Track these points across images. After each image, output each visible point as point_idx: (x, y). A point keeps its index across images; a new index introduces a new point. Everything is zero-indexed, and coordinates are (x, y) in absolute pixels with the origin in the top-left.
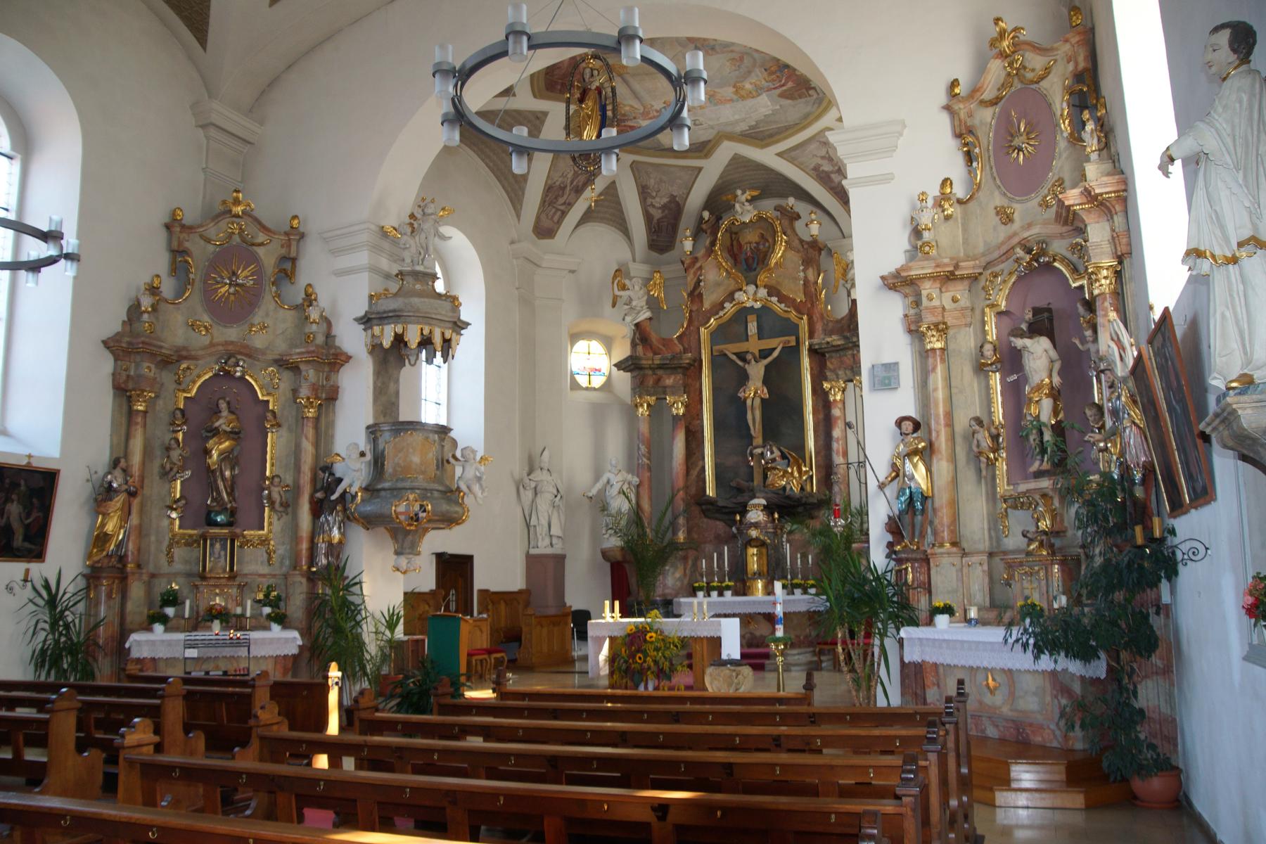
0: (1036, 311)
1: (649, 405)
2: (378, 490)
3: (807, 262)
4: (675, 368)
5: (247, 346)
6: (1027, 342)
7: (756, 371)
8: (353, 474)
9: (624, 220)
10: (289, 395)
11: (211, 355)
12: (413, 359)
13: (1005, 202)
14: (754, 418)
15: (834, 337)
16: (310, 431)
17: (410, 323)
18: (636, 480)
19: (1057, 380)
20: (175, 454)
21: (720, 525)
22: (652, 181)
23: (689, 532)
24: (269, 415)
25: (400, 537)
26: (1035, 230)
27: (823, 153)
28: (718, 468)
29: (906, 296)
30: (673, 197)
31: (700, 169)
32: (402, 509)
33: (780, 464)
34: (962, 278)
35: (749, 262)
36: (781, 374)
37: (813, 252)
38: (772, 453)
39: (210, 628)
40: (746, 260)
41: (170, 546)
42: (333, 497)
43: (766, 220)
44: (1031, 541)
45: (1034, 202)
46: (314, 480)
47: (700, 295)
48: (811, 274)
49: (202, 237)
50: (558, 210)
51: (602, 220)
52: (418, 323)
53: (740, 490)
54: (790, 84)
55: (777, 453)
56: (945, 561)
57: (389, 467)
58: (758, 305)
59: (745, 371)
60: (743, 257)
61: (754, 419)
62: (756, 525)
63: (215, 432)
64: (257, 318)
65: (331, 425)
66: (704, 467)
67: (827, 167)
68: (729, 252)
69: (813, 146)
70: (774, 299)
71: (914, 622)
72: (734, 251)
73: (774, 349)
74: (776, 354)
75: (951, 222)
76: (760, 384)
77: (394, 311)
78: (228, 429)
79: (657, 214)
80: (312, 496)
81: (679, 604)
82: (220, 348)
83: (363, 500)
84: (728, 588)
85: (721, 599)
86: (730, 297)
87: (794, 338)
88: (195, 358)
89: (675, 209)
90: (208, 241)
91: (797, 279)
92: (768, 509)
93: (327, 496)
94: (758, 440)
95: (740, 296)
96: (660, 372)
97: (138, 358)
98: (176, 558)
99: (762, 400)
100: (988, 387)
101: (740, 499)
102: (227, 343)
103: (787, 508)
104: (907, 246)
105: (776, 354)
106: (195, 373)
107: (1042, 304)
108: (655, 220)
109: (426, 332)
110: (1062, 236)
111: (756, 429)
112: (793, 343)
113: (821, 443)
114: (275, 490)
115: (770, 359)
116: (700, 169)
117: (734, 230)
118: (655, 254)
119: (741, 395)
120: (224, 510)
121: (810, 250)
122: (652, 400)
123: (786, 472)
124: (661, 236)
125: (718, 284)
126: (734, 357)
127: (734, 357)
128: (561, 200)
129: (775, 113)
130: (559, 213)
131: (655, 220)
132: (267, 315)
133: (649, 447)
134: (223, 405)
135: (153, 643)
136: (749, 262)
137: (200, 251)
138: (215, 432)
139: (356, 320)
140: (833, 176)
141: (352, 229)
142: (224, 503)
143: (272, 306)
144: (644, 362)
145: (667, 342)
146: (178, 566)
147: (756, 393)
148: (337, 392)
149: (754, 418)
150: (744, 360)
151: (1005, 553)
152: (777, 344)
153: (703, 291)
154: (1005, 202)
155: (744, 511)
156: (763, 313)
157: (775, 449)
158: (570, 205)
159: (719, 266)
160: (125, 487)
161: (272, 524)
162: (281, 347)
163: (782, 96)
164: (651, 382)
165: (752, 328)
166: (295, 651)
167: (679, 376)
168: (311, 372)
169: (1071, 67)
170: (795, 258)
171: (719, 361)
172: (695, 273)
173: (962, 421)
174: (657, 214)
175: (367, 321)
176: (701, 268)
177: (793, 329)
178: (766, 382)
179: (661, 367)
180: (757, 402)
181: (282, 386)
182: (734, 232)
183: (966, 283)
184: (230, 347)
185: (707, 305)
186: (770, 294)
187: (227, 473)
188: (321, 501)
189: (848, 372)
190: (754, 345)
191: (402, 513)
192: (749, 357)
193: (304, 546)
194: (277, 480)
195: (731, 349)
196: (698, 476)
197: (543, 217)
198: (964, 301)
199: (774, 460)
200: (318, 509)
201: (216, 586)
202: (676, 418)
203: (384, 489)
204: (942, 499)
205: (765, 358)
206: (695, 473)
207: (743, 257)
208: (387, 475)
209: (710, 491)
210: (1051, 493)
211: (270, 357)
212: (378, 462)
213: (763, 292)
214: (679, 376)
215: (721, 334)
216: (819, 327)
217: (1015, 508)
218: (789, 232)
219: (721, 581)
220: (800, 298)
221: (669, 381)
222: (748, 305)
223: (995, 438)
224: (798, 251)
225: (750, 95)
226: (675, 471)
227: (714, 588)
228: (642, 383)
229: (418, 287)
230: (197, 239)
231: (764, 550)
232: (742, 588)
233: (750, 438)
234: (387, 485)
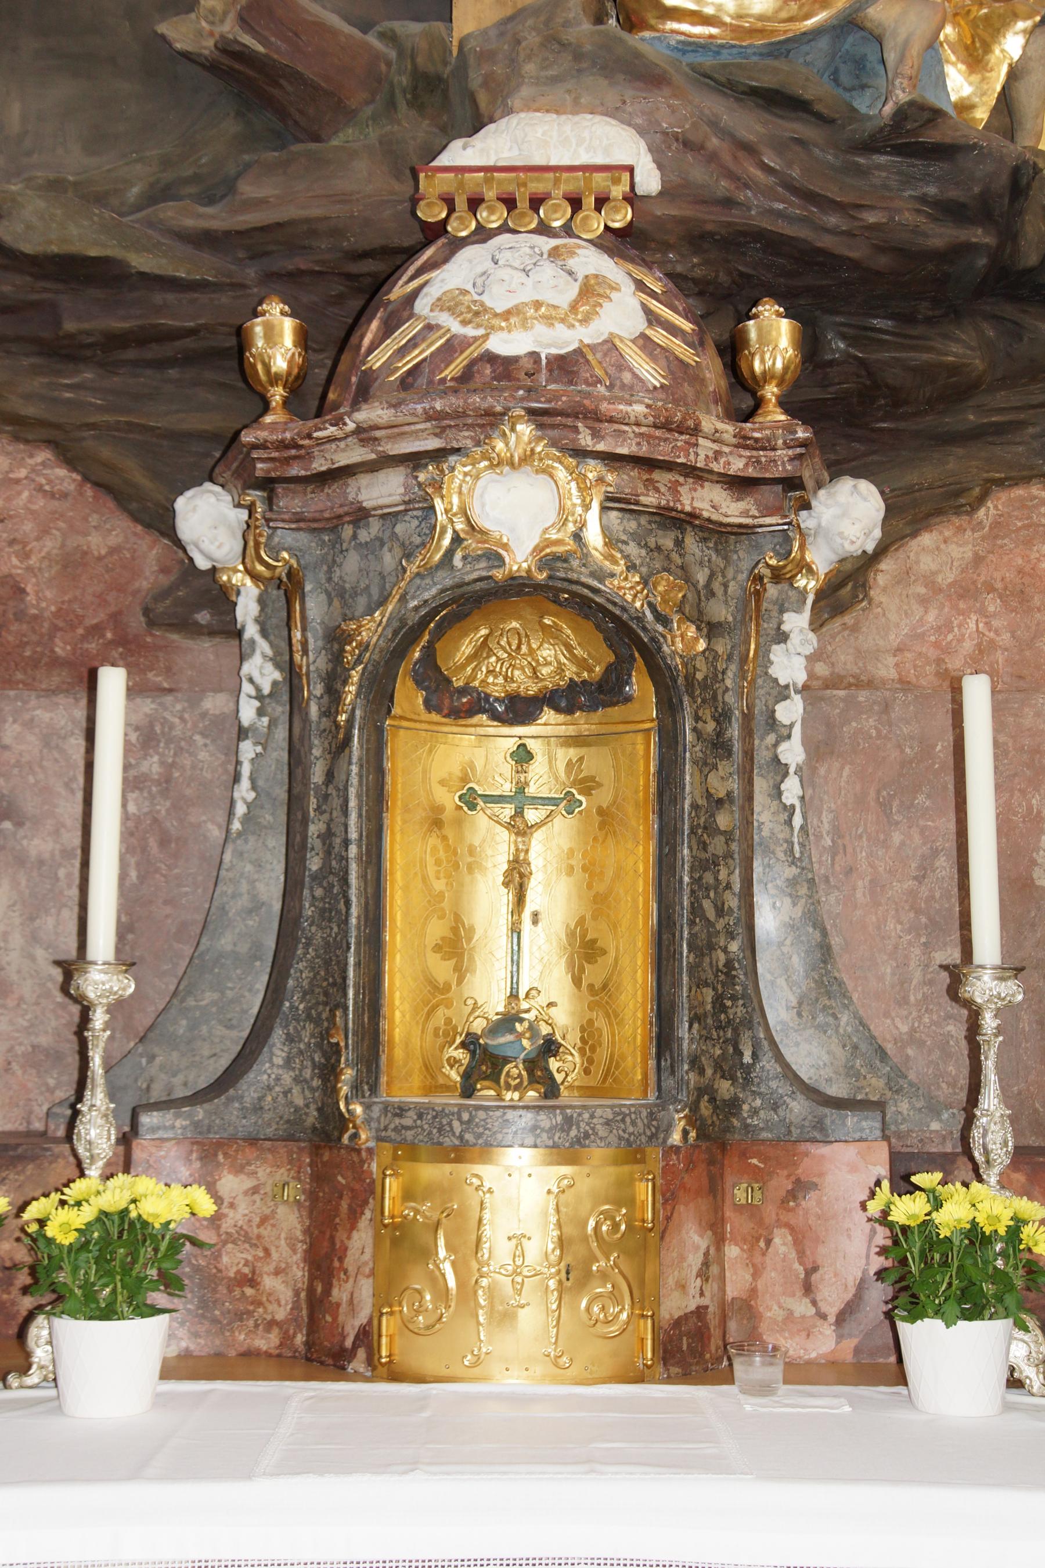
101: (269, 195)
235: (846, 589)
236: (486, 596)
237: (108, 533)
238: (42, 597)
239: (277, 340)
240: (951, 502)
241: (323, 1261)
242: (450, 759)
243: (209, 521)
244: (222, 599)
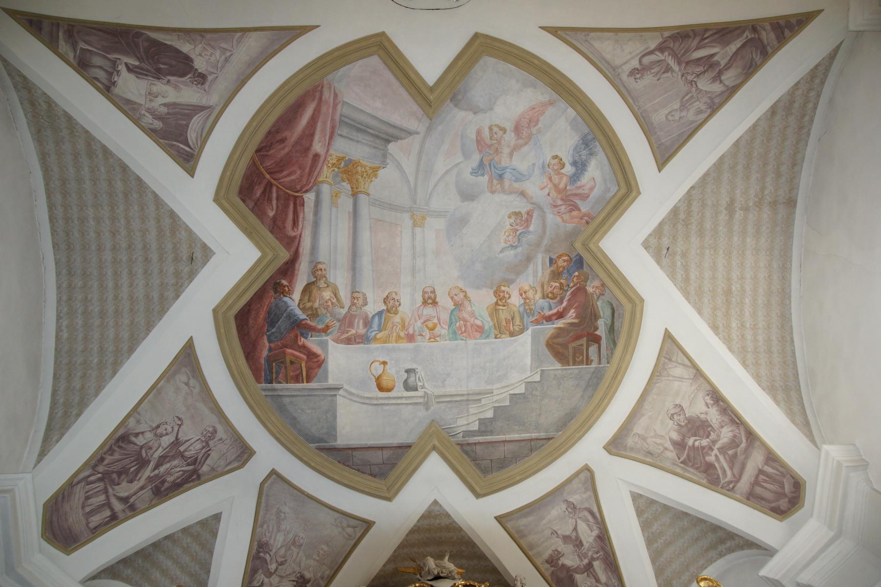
22: (280, 538)
27: (567, 530)
50: (108, 504)
67: (570, 560)
69: (557, 511)
128: (124, 489)
130: (108, 513)
140: (578, 577)
158: (133, 510)
197: (79, 493)
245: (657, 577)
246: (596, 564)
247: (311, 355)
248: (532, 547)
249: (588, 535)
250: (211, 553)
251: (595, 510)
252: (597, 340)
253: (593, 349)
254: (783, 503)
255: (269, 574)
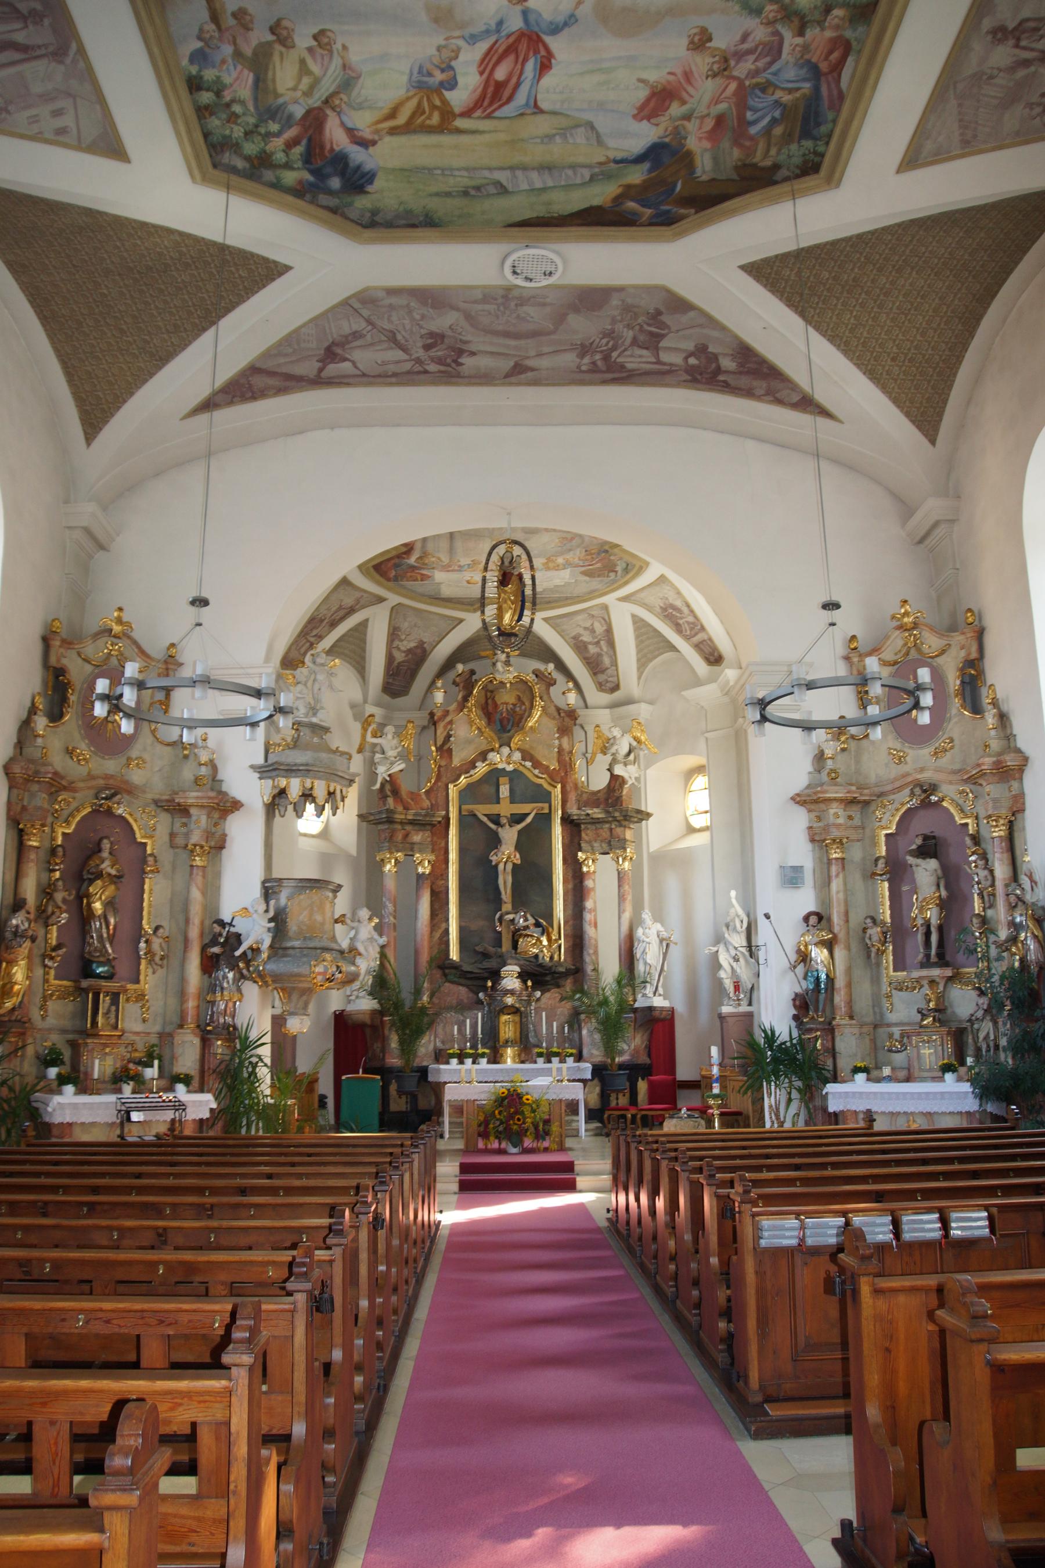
0: (926, 838)
1: (396, 860)
2: (286, 948)
3: (564, 731)
4: (424, 825)
5: (127, 782)
6: (919, 861)
7: (509, 835)
8: (255, 931)
9: (363, 658)
10: (166, 838)
11: (89, 788)
12: (282, 809)
13: (898, 746)
14: (505, 882)
15: (596, 810)
16: (199, 879)
17: (319, 778)
18: (383, 941)
19: (944, 893)
20: (59, 896)
21: (463, 990)
22: (406, 624)
23: (431, 996)
24: (150, 859)
25: (295, 997)
26: (927, 776)
27: (588, 624)
28: (462, 930)
29: (810, 811)
30: (422, 643)
31: (461, 621)
32: (319, 969)
33: (536, 932)
34: (859, 802)
35: (505, 723)
36: (533, 839)
37: (567, 720)
38: (526, 920)
39: (119, 1091)
40: (501, 721)
41: (45, 999)
42: (237, 953)
43: (526, 683)
44: (924, 1016)
45: (926, 752)
46: (202, 934)
47: (450, 751)
48: (565, 742)
49: (79, 654)
51: (341, 655)
52: (327, 780)
53: (486, 955)
54: (599, 565)
55: (531, 921)
56: (847, 1030)
57: (293, 926)
58: (510, 768)
59: (496, 834)
60: (498, 716)
61: (505, 883)
62: (512, 992)
63: (99, 875)
64: (134, 753)
65: (218, 875)
66: (446, 932)
67: (586, 638)
68: (483, 709)
69: (579, 617)
70: (528, 764)
71: (835, 1079)
72: (489, 709)
73: (528, 815)
74: (529, 819)
75: (846, 753)
76: (512, 849)
77: (307, 765)
78: (113, 872)
79: (399, 657)
80: (204, 949)
81: (438, 1071)
82: (101, 782)
83: (269, 958)
84: (483, 1055)
85: (548, 1065)
86: (483, 756)
87: (546, 805)
88: (74, 790)
89: (419, 655)
90: (86, 660)
91: (550, 746)
92: (523, 976)
93: (222, 951)
94: (507, 907)
95: (491, 755)
96: (408, 828)
97: (35, 787)
98: (50, 1012)
99: (514, 864)
100: (874, 892)
101: (487, 964)
102: (107, 777)
103: (538, 975)
104: (810, 769)
105: (529, 819)
106: (74, 805)
107: (927, 832)
108: (396, 663)
109: (308, 785)
110: (951, 783)
111: (506, 895)
112: (546, 811)
113: (570, 912)
114: (156, 943)
115: (523, 824)
116: (461, 621)
117: (490, 687)
118: (387, 698)
119: (494, 859)
120: (108, 962)
121: (567, 719)
122: (399, 855)
123: (538, 939)
124: (399, 678)
125: (469, 742)
126: (485, 819)
127: (485, 819)
128: (314, 633)
129: (567, 584)
130: (308, 644)
131: (396, 663)
132: (145, 749)
133: (395, 906)
134: (106, 845)
135: (75, 1106)
136: (505, 723)
137: (76, 670)
138: (99, 875)
139: (252, 767)
140: (590, 647)
141: (250, 671)
142: (109, 955)
143: (150, 739)
144: (397, 816)
145: (414, 796)
146: (51, 1021)
147: (509, 857)
148: (224, 841)
149: (505, 882)
150: (498, 823)
151: (889, 1025)
152: (530, 809)
153: (453, 746)
154: (898, 746)
155: (496, 975)
156: (515, 776)
157: (529, 916)
159: (471, 723)
160: (30, 933)
161: (150, 980)
162: (158, 788)
163: (584, 573)
164: (399, 836)
165: (504, 791)
166: (206, 1115)
167: (428, 834)
168: (204, 819)
169: (963, 653)
170: (551, 726)
171: (468, 821)
172: (445, 727)
173: (857, 917)
174: (399, 657)
175: (267, 770)
176: (451, 722)
177: (546, 797)
178: (518, 847)
179: (412, 823)
180: (510, 866)
181: (159, 827)
182: (491, 691)
183: (860, 806)
184: (111, 782)
185: (456, 762)
186: (524, 759)
187: (112, 921)
188: (217, 956)
189: (604, 845)
190: (505, 809)
191: (319, 974)
192: (504, 821)
193: (191, 1004)
194: (161, 931)
195: (482, 810)
196: (440, 939)
198: (857, 821)
199: (526, 928)
200: (210, 965)
201: (106, 1045)
202: (420, 877)
203: (293, 948)
204: (840, 983)
205: (518, 822)
206: (437, 935)
207: (498, 716)
208: (291, 934)
209: (454, 955)
210: (938, 980)
211: (149, 796)
212: (279, 921)
213: (517, 756)
214: (428, 834)
215: (469, 794)
216: (572, 797)
217: (901, 990)
218: (545, 697)
219: (474, 1047)
220: (554, 765)
221: (417, 838)
222: (500, 766)
223: (884, 933)
224: (554, 718)
225: (557, 568)
226: (419, 932)
227: (469, 1056)
228: (391, 837)
229: (316, 740)
230: (73, 654)
231: (517, 1018)
232: (495, 1058)
233: (498, 901)
234: (297, 944)
235: (538, 1000)
236: (507, 1007)
237: (471, 995)
238: (465, 1001)
239: (490, 984)
240: (549, 990)
241: (495, 1057)
242: (504, 1018)
243: (481, 995)
244: (482, 1003)
245: (638, 653)
246: (602, 643)
247: (422, 575)
248: (563, 631)
249: (599, 628)
250: (365, 635)
251: (607, 618)
252: (616, 572)
253: (612, 575)
254: (712, 659)
255: (402, 641)
